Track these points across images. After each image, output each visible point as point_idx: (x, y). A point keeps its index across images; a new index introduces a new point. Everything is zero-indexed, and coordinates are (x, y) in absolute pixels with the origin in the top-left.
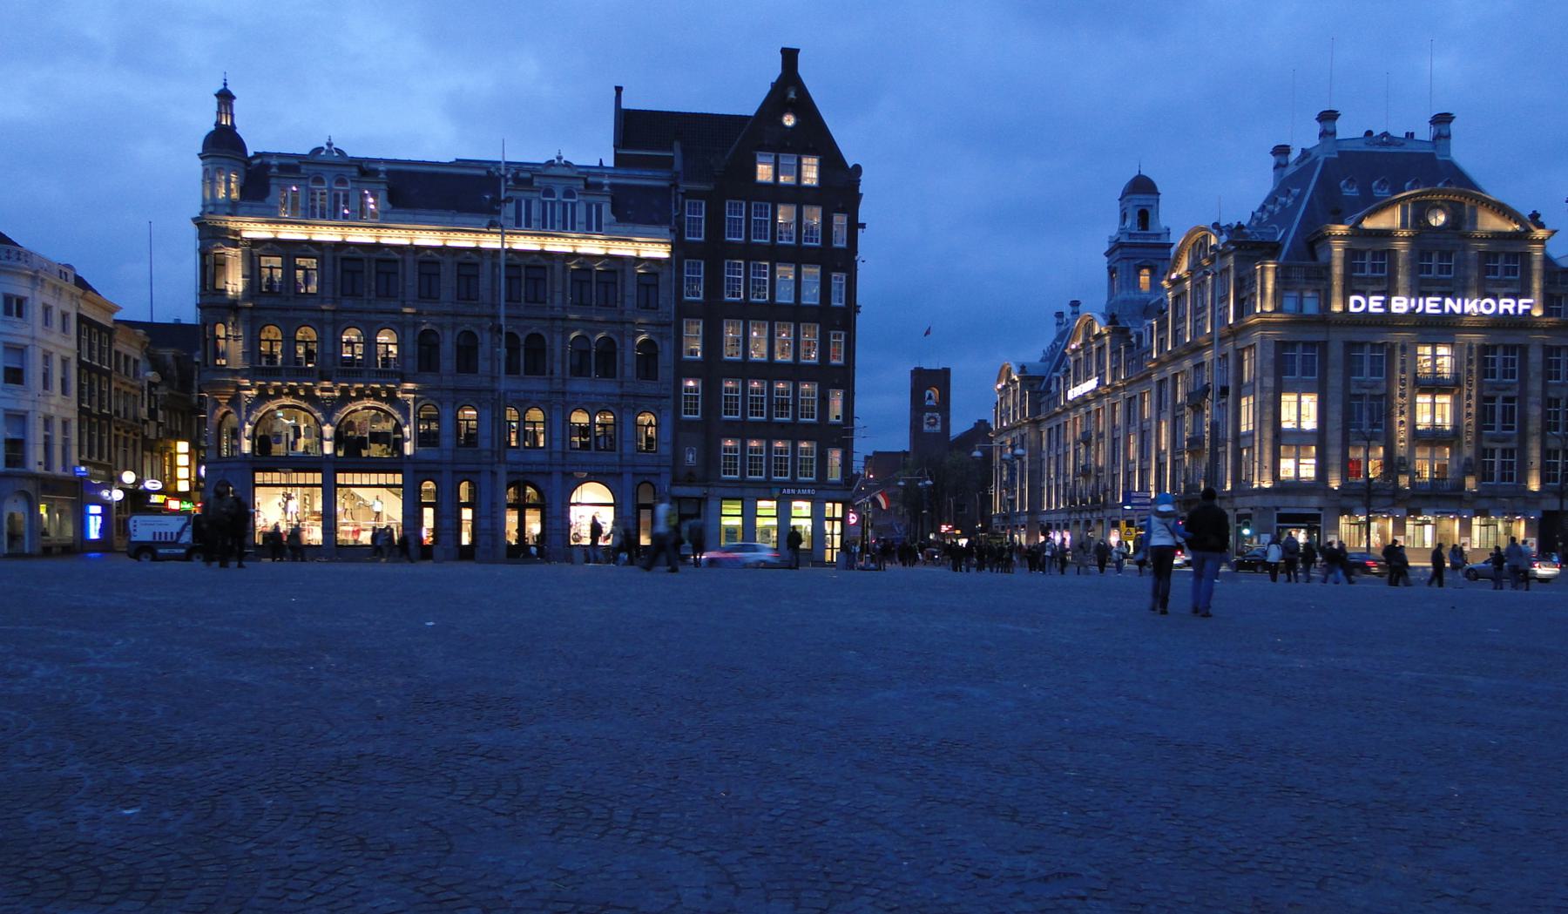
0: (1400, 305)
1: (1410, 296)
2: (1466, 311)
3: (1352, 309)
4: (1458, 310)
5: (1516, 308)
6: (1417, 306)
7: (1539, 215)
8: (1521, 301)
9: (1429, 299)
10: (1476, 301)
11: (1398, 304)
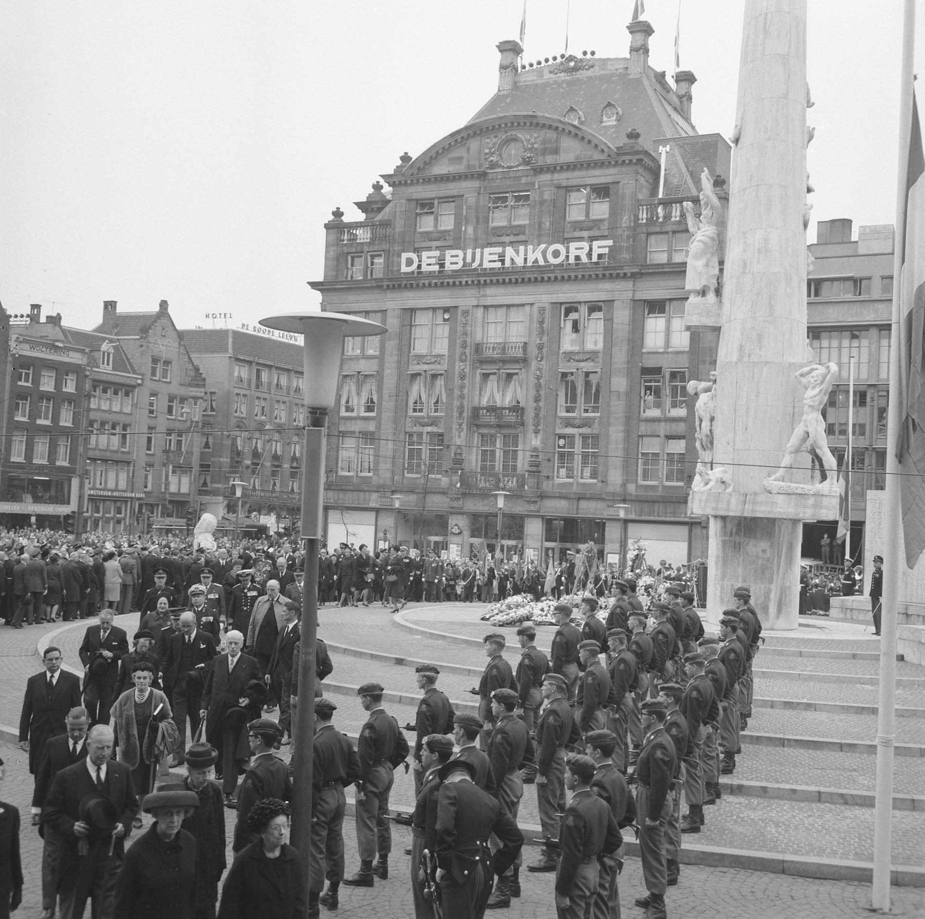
2: (529, 264)
3: (404, 269)
4: (520, 262)
5: (589, 255)
6: (473, 260)
7: (637, 136)
8: (596, 244)
9: (487, 250)
10: (543, 246)
11: (454, 260)
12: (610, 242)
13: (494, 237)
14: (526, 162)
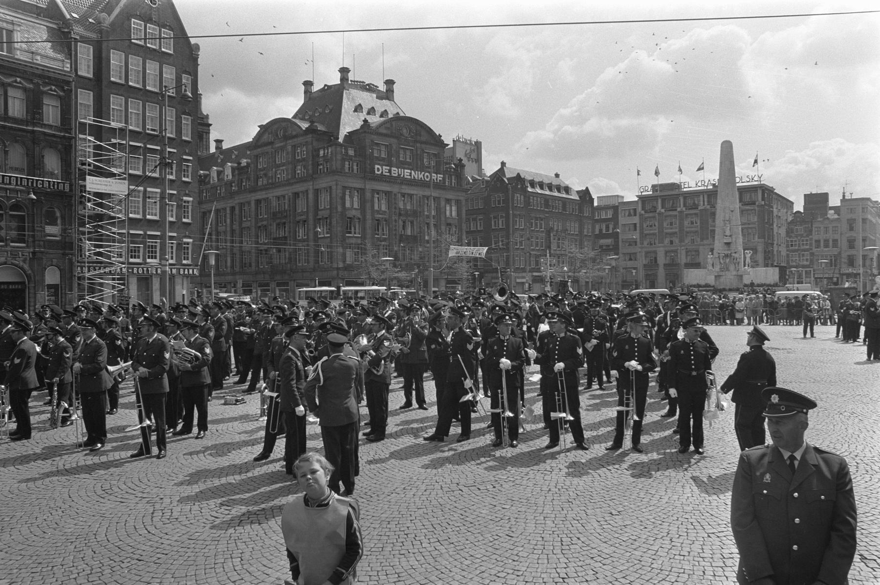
0: (395, 171)
1: (398, 168)
3: (376, 172)
4: (416, 177)
8: (439, 175)
9: (406, 171)
12: (442, 176)
13: (402, 165)
14: (412, 137)
